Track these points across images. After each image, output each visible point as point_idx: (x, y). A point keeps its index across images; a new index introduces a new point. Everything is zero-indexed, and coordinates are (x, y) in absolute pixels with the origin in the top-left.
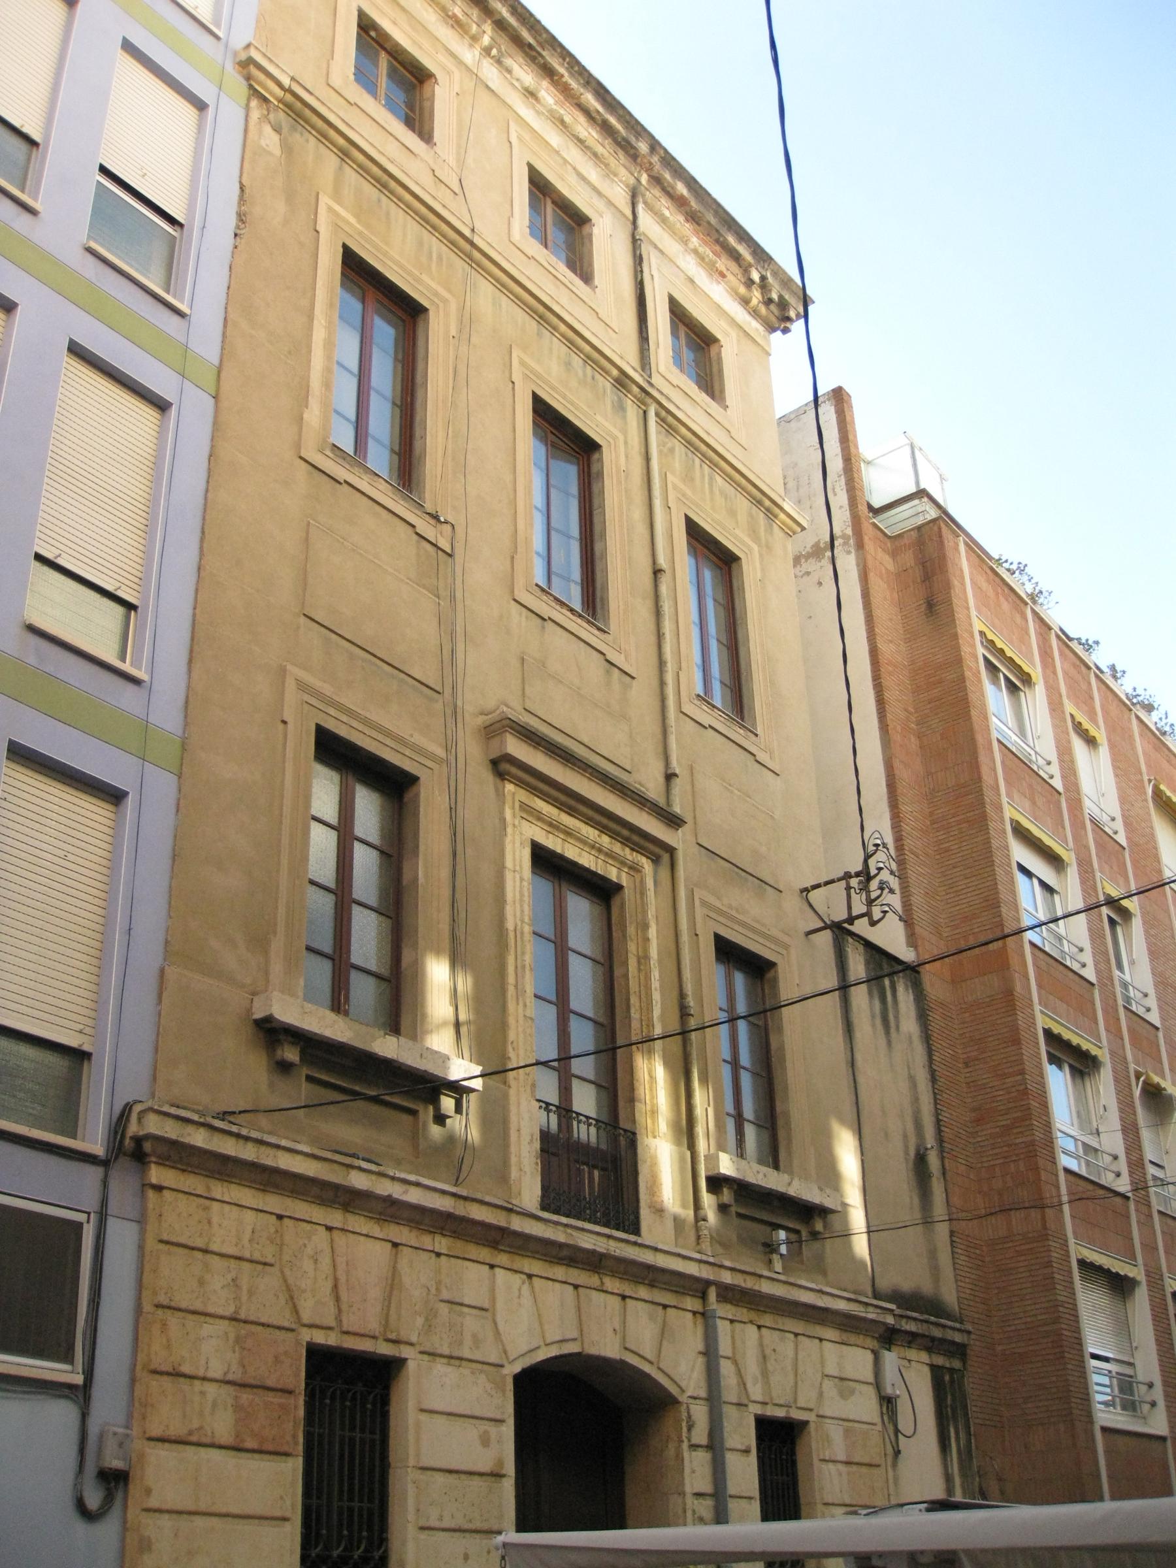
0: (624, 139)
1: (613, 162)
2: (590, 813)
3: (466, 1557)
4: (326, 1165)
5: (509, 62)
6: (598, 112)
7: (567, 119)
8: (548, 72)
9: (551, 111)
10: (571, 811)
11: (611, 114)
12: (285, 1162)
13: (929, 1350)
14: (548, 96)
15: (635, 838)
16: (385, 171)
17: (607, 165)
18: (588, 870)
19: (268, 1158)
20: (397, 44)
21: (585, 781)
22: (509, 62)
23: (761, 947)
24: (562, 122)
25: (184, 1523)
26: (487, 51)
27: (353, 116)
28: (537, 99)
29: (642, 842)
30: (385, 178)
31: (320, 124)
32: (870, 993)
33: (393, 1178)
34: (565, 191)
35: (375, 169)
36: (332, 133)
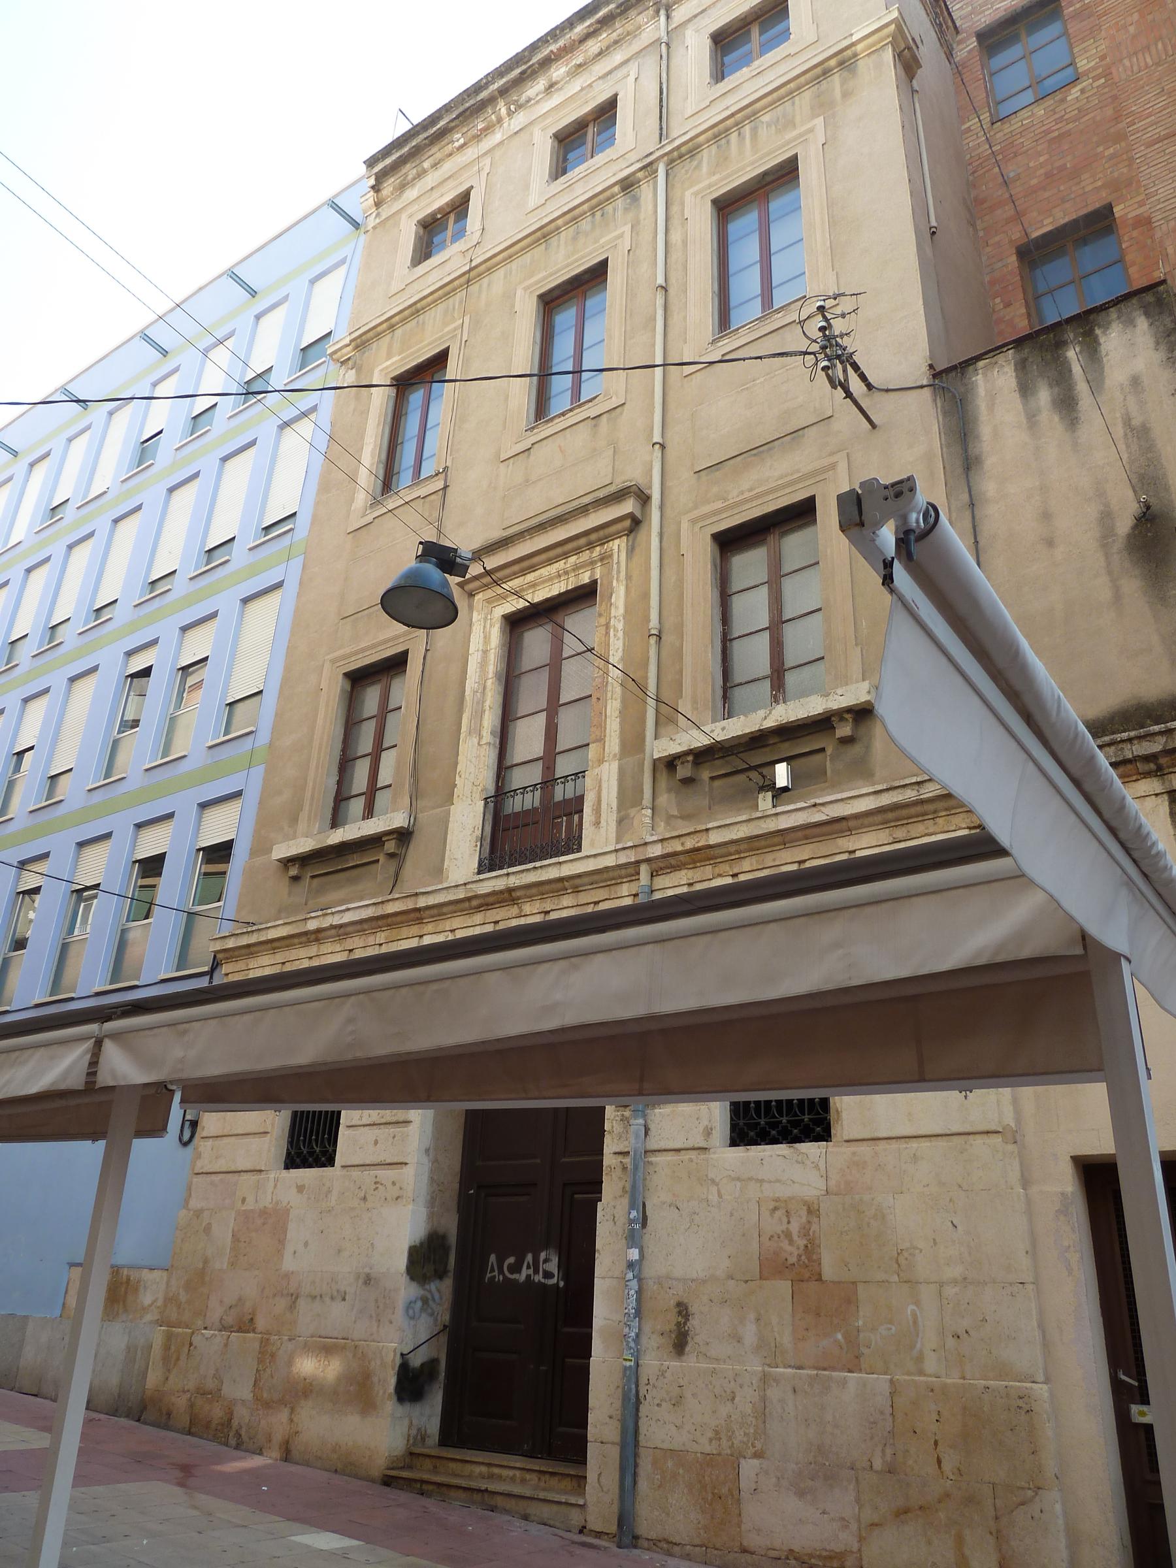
0: (617, 7)
1: (629, 27)
2: (543, 557)
3: (376, 1142)
4: (294, 925)
5: (524, 98)
6: (591, 25)
7: (580, 60)
8: (547, 62)
9: (568, 73)
10: (533, 568)
11: (600, 10)
12: (273, 934)
13: (1159, 773)
14: (558, 71)
15: (593, 537)
16: (410, 306)
17: (628, 34)
18: (560, 595)
19: (263, 937)
20: (447, 204)
21: (582, 520)
22: (524, 98)
23: (785, 498)
24: (580, 66)
25: (218, 1142)
26: (510, 113)
27: (431, 278)
28: (556, 83)
29: (601, 533)
30: (413, 308)
31: (371, 334)
32: (1025, 389)
33: (333, 913)
34: (587, 108)
35: (406, 313)
36: (379, 329)
